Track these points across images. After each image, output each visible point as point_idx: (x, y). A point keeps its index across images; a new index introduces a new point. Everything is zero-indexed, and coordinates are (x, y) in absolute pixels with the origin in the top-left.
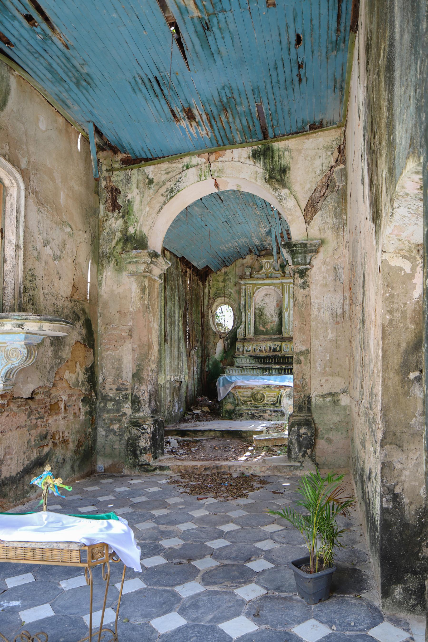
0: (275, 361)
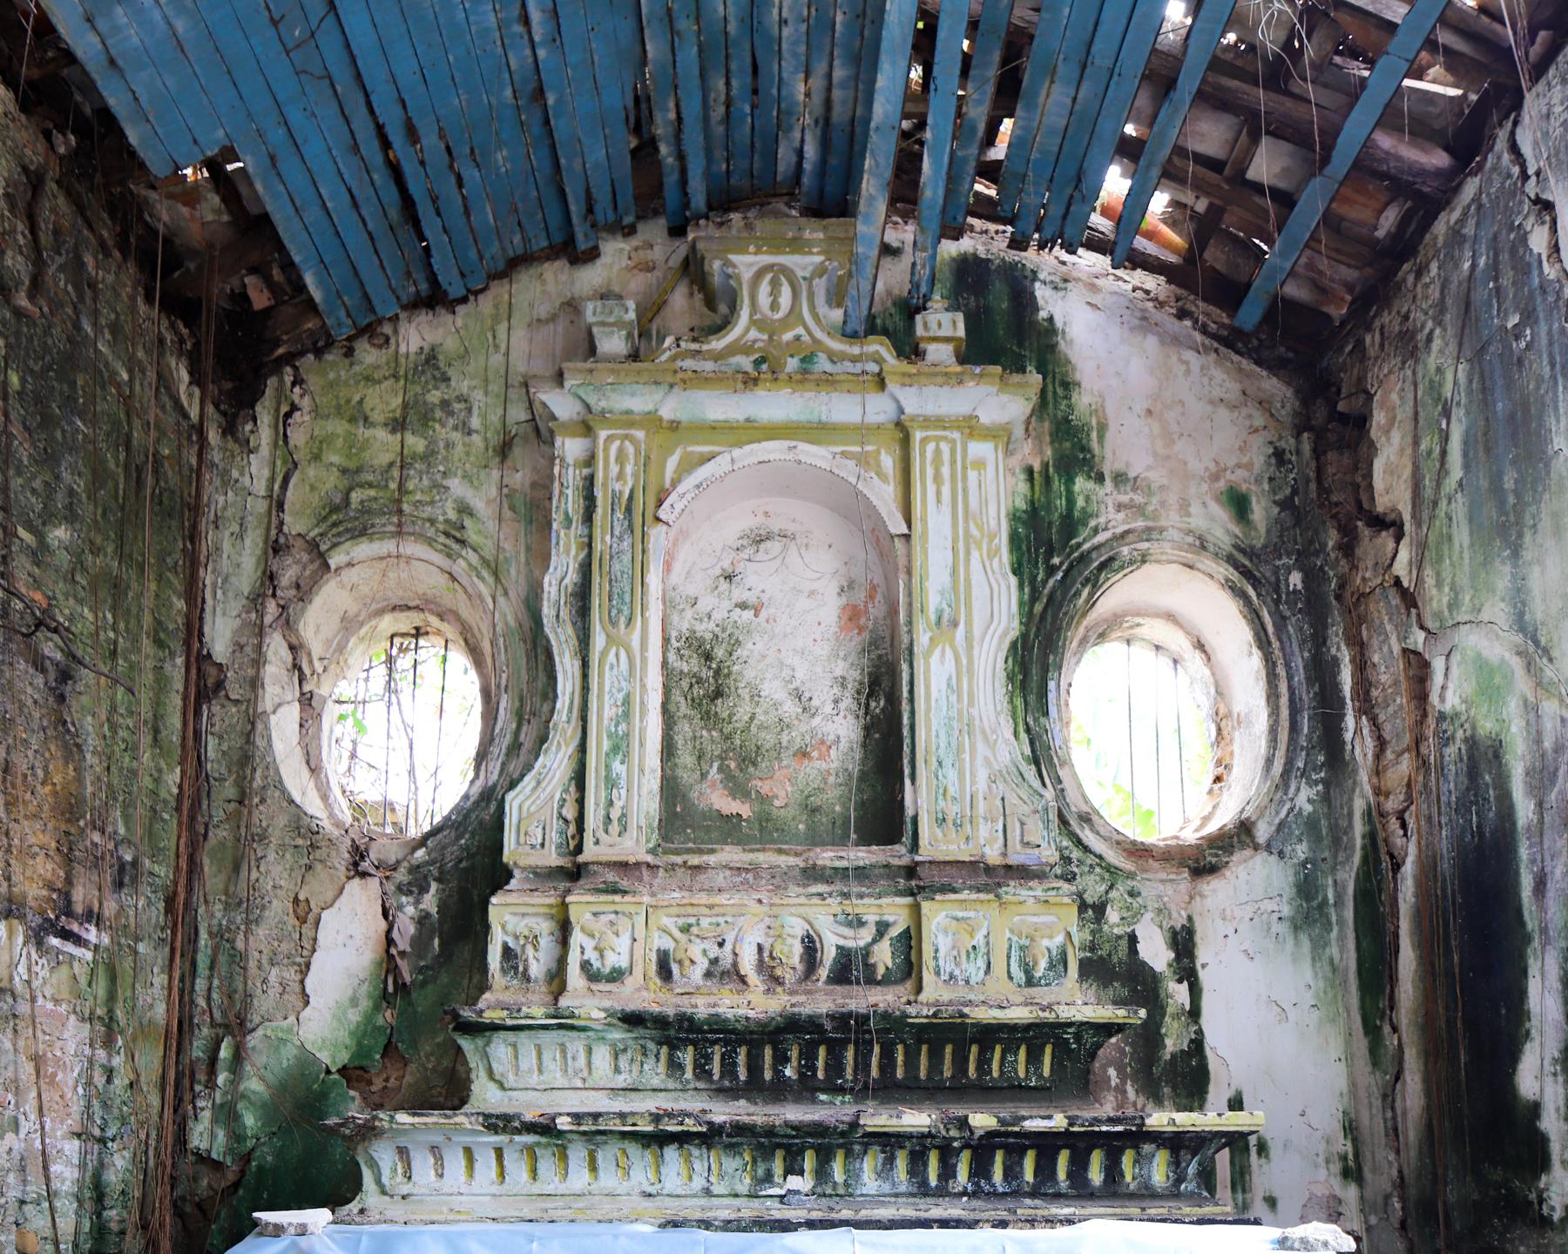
0: (862, 1065)
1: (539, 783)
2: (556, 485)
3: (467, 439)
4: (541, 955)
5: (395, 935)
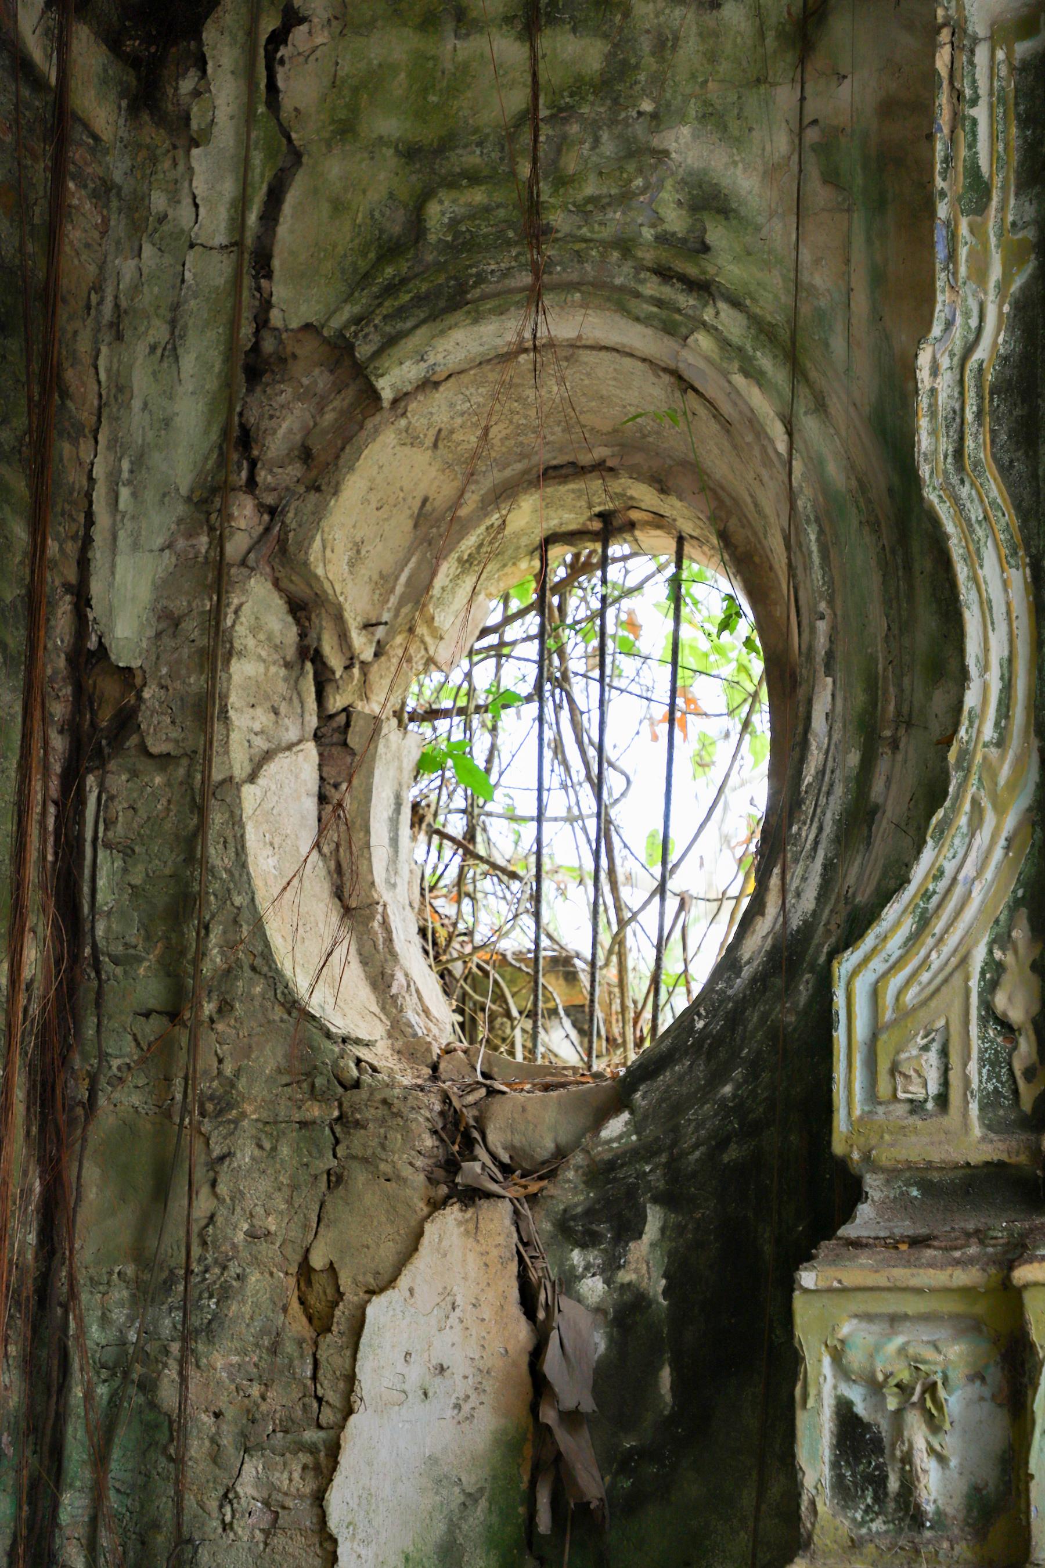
1: (924, 922)
2: (944, 99)
3: (710, 19)
4: (951, 1443)
5: (552, 1363)
